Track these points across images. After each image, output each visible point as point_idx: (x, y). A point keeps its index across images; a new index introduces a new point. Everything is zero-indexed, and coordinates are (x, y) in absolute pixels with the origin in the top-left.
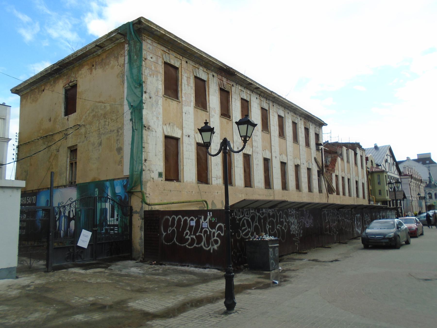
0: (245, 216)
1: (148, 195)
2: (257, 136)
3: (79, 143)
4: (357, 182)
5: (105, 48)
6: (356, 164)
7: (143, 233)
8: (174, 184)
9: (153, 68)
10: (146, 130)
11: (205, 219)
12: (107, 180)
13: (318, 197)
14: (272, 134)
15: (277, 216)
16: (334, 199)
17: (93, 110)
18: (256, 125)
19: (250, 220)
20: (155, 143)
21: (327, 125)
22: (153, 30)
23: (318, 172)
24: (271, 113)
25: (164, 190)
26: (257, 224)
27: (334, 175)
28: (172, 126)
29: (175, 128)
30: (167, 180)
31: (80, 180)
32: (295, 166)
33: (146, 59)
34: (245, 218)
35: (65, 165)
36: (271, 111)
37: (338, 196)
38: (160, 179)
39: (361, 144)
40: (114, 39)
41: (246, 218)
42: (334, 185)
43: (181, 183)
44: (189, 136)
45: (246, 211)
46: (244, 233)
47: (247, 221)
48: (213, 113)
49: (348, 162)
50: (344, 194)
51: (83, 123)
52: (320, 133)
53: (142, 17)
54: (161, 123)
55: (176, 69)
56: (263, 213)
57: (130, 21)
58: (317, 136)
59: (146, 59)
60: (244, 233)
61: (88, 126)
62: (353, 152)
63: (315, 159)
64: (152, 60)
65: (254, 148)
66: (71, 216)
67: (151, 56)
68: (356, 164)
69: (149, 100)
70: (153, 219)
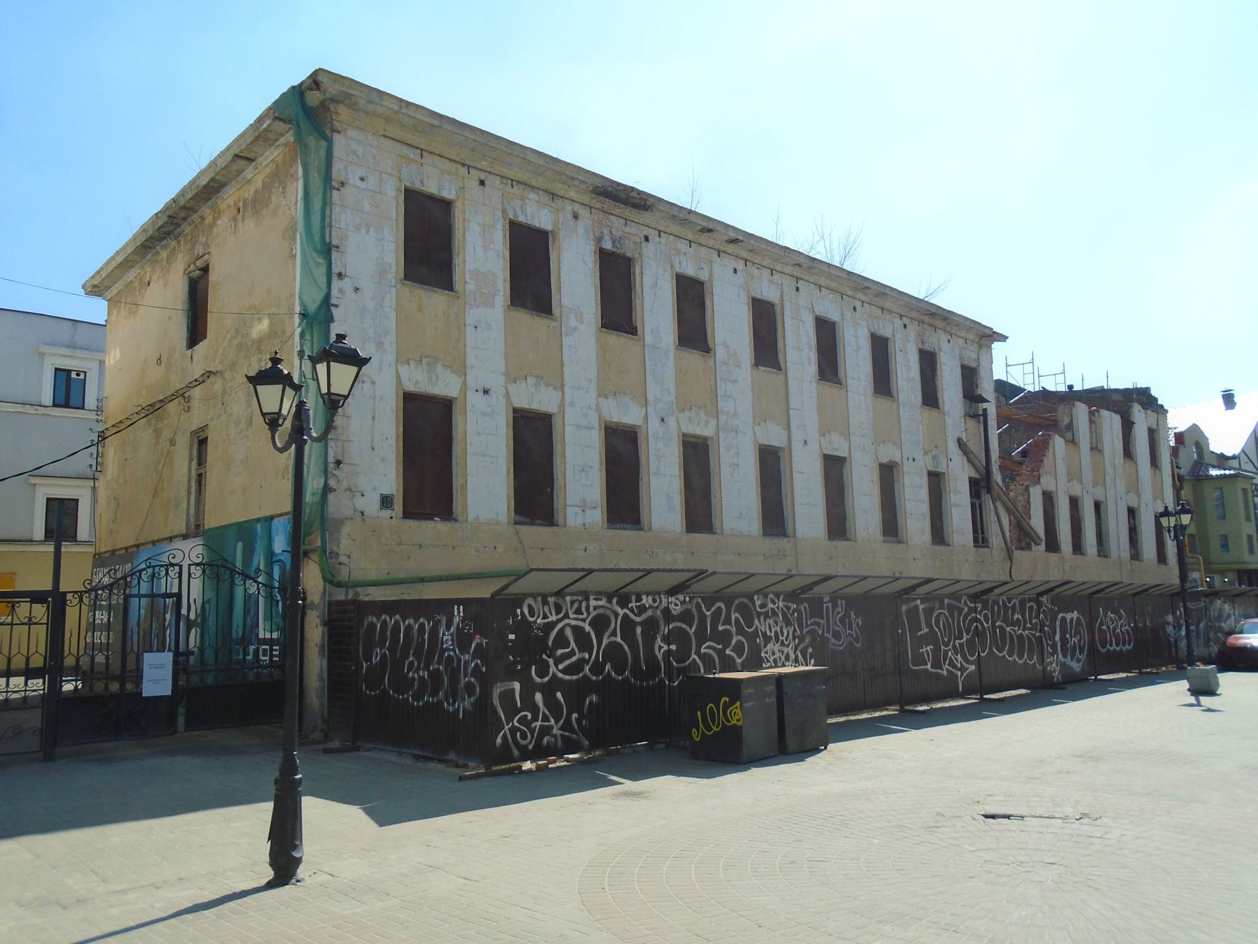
0: (566, 616)
1: (343, 559)
2: (735, 382)
3: (212, 419)
4: (1132, 512)
6: (1128, 453)
7: (325, 662)
8: (437, 527)
9: (367, 208)
11: (448, 627)
12: (258, 520)
13: (971, 559)
14: (790, 375)
15: (703, 618)
16: (1037, 567)
17: (237, 331)
18: (366, 361)
19: (587, 628)
21: (1003, 338)
23: (974, 483)
24: (787, 313)
25: (400, 544)
26: (618, 639)
27: (1036, 494)
28: (428, 364)
29: (439, 368)
30: (407, 515)
31: (212, 521)
32: (881, 465)
33: (343, 184)
34: (567, 621)
35: (186, 480)
36: (787, 305)
37: (1053, 556)
38: (388, 513)
39: (1154, 393)
40: (271, 136)
41: (574, 623)
42: (1037, 522)
43: (458, 525)
44: (486, 392)
45: (572, 603)
46: (561, 667)
47: (578, 631)
48: (573, 322)
49: (1096, 448)
50: (1078, 547)
51: (220, 368)
52: (983, 363)
53: (321, 69)
54: (391, 358)
55: (447, 205)
56: (642, 609)
57: (296, 83)
58: (970, 376)
59: (343, 184)
60: (561, 667)
61: (227, 375)
62: (1117, 419)
63: (960, 443)
64: (363, 185)
65: (722, 419)
66: (192, 616)
67: (361, 173)
68: (1128, 453)
69: (350, 294)
70: (346, 621)
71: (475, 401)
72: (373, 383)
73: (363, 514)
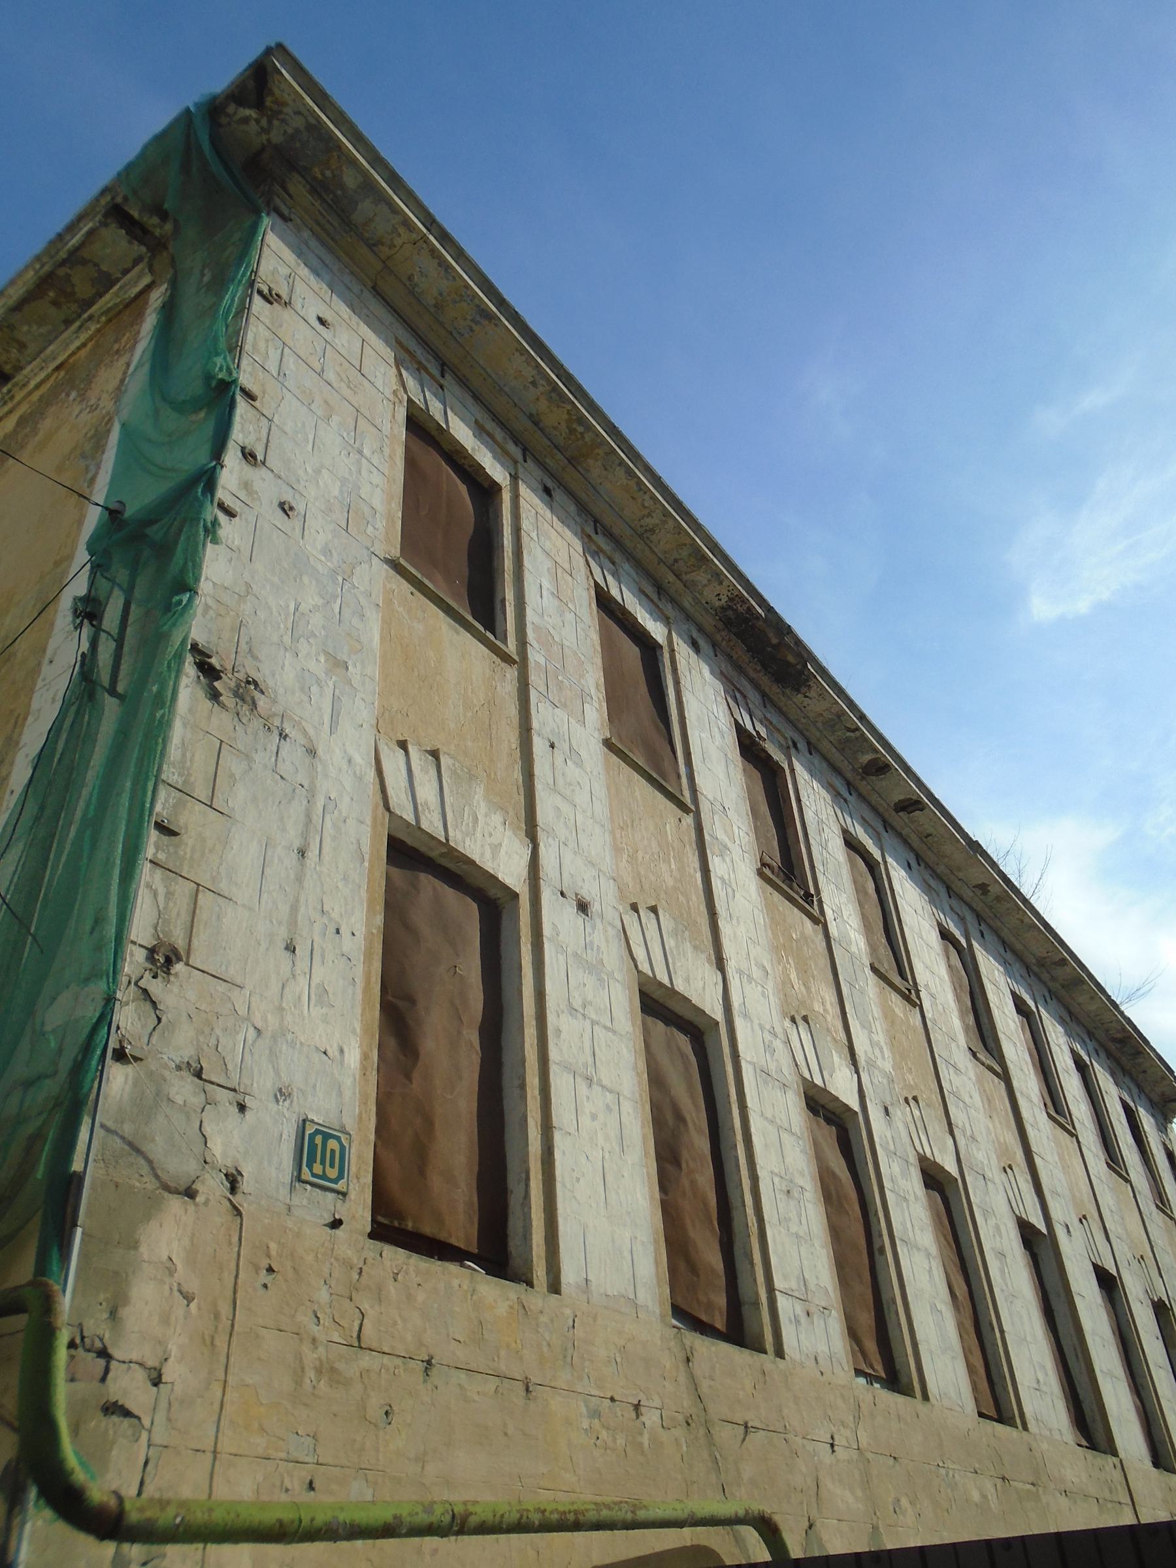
1: (128, 1386)
5: (19, 378)
10: (215, 696)
20: (293, 836)
22: (350, 180)
25: (359, 1343)
28: (454, 773)
44: (583, 907)
54: (361, 710)
71: (558, 918)
72: (312, 752)
73: (233, 1181)
